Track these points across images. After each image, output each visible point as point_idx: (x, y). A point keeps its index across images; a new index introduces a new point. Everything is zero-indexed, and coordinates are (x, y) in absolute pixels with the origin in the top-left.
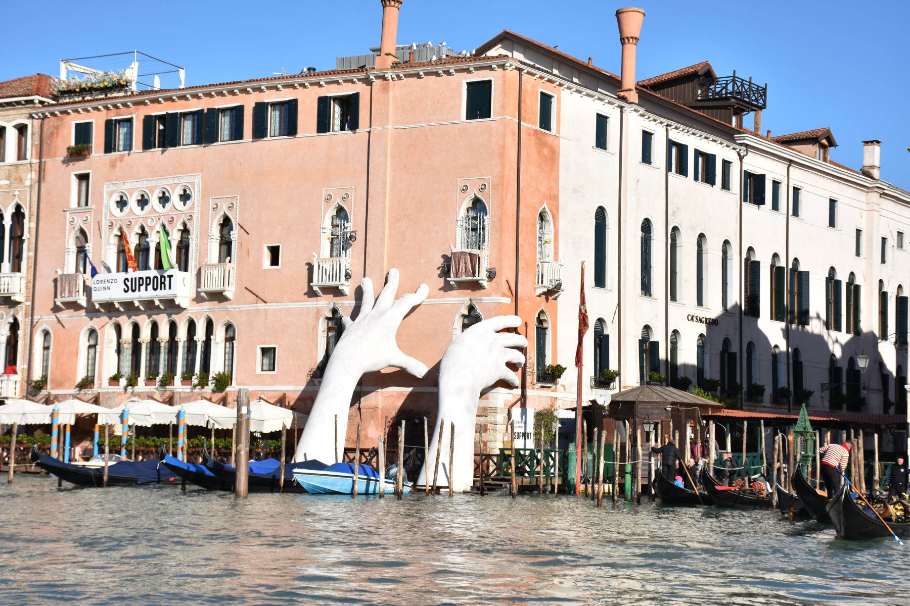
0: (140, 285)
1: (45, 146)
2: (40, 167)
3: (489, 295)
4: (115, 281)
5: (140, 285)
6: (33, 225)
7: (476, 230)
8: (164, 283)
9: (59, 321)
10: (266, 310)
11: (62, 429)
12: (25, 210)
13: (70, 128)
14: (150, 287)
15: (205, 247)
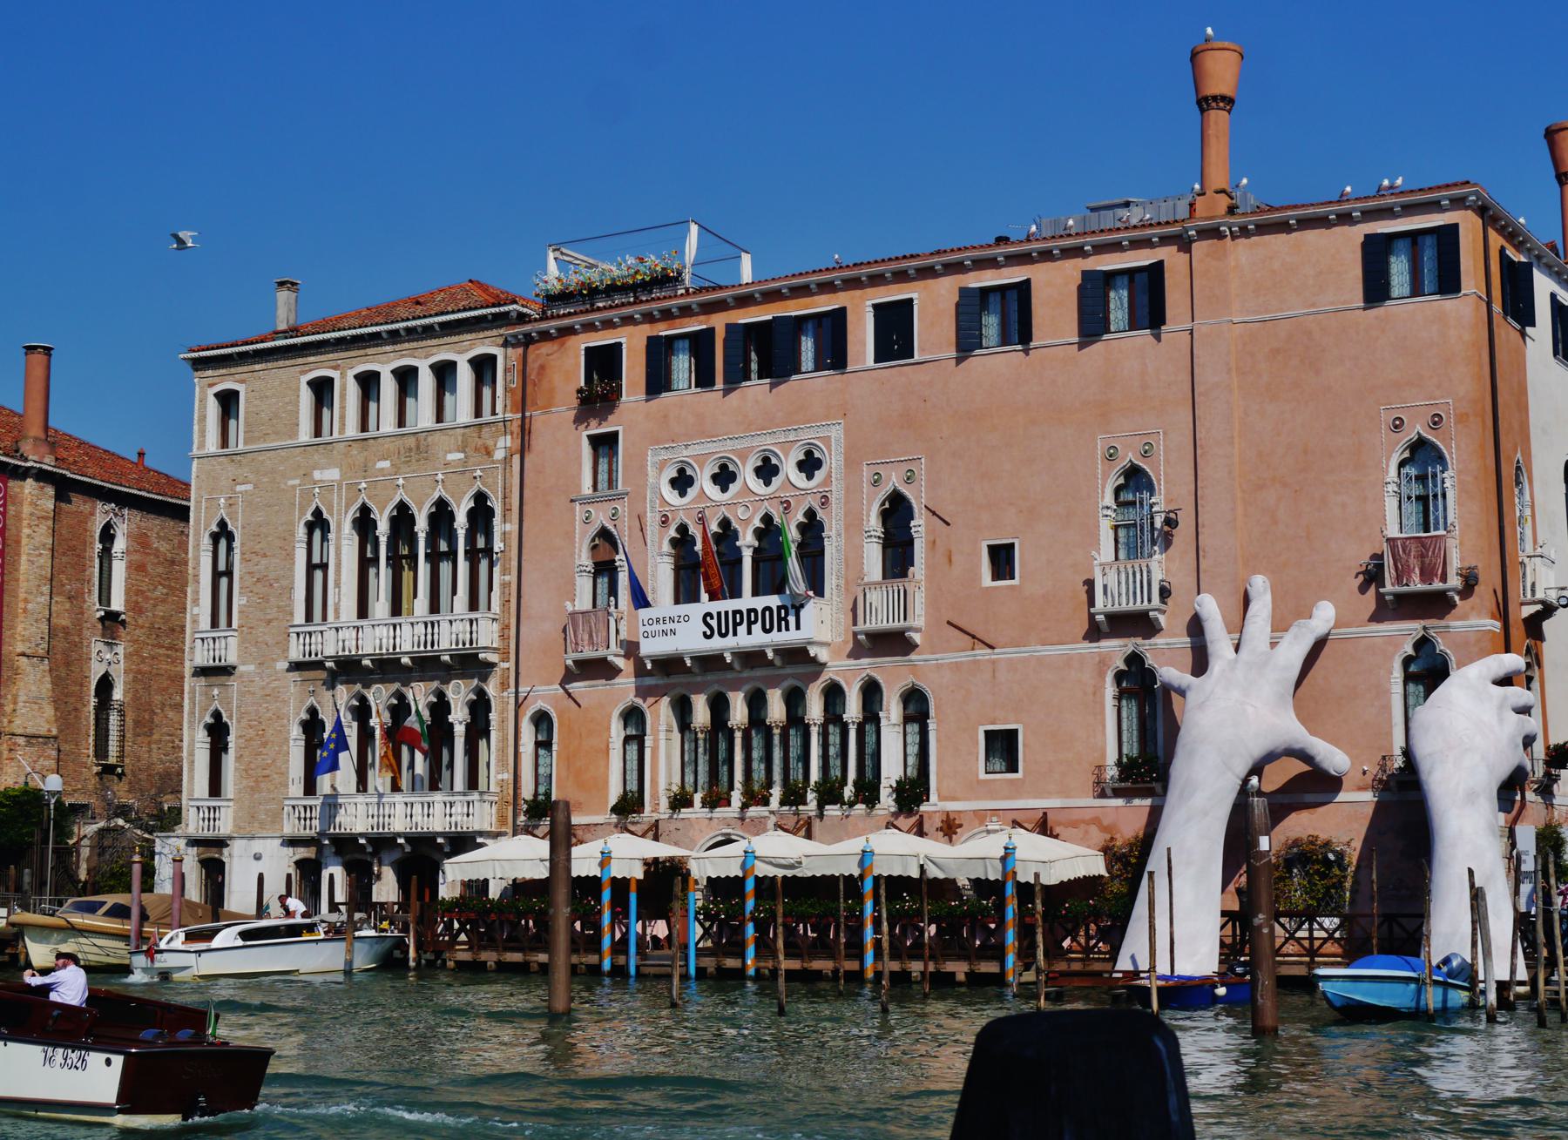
0: (736, 625)
1: (529, 389)
2: (522, 427)
3: (1464, 617)
4: (687, 619)
5: (736, 625)
6: (512, 527)
7: (1426, 504)
8: (785, 619)
9: (569, 695)
10: (993, 662)
11: (620, 886)
12: (496, 504)
13: (578, 356)
14: (757, 628)
15: (853, 549)
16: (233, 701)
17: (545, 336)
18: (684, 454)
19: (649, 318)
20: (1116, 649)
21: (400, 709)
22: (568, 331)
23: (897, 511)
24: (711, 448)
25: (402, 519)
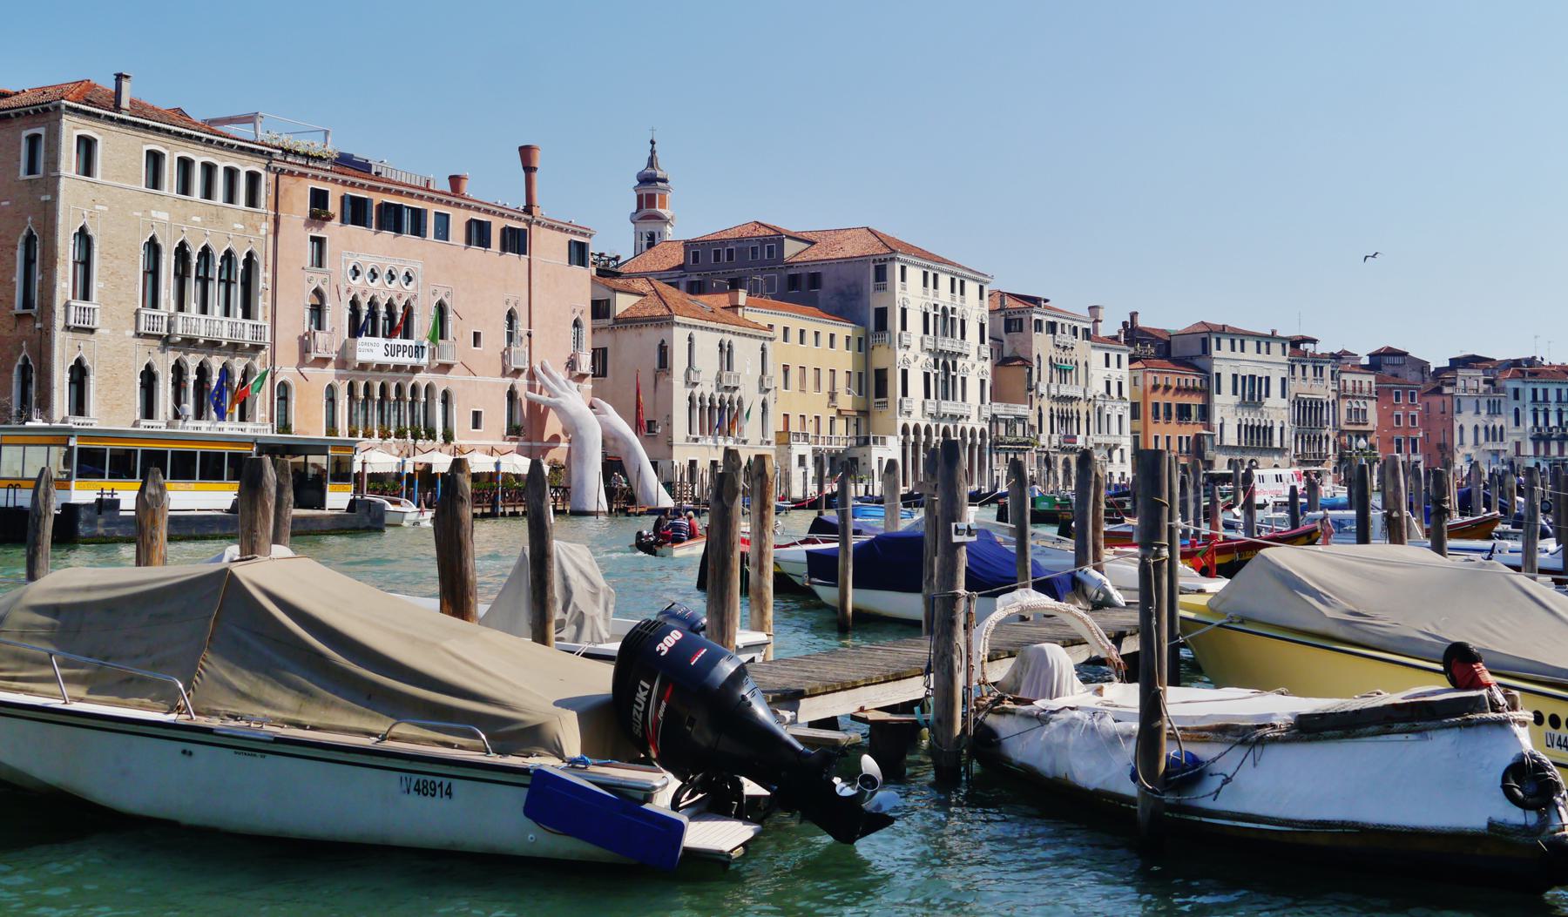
6: (269, 275)
15: (423, 323)
16: (89, 350)
17: (291, 173)
18: (358, 259)
19: (344, 183)
20: (509, 381)
21: (202, 371)
22: (304, 175)
23: (441, 309)
24: (367, 259)
25: (206, 253)
